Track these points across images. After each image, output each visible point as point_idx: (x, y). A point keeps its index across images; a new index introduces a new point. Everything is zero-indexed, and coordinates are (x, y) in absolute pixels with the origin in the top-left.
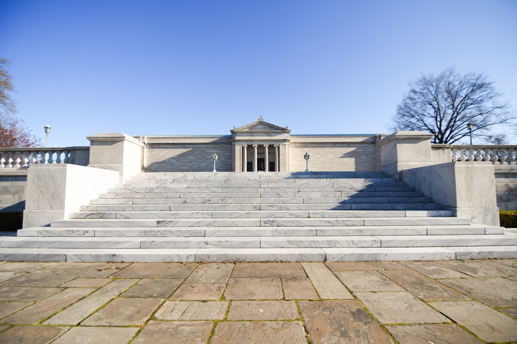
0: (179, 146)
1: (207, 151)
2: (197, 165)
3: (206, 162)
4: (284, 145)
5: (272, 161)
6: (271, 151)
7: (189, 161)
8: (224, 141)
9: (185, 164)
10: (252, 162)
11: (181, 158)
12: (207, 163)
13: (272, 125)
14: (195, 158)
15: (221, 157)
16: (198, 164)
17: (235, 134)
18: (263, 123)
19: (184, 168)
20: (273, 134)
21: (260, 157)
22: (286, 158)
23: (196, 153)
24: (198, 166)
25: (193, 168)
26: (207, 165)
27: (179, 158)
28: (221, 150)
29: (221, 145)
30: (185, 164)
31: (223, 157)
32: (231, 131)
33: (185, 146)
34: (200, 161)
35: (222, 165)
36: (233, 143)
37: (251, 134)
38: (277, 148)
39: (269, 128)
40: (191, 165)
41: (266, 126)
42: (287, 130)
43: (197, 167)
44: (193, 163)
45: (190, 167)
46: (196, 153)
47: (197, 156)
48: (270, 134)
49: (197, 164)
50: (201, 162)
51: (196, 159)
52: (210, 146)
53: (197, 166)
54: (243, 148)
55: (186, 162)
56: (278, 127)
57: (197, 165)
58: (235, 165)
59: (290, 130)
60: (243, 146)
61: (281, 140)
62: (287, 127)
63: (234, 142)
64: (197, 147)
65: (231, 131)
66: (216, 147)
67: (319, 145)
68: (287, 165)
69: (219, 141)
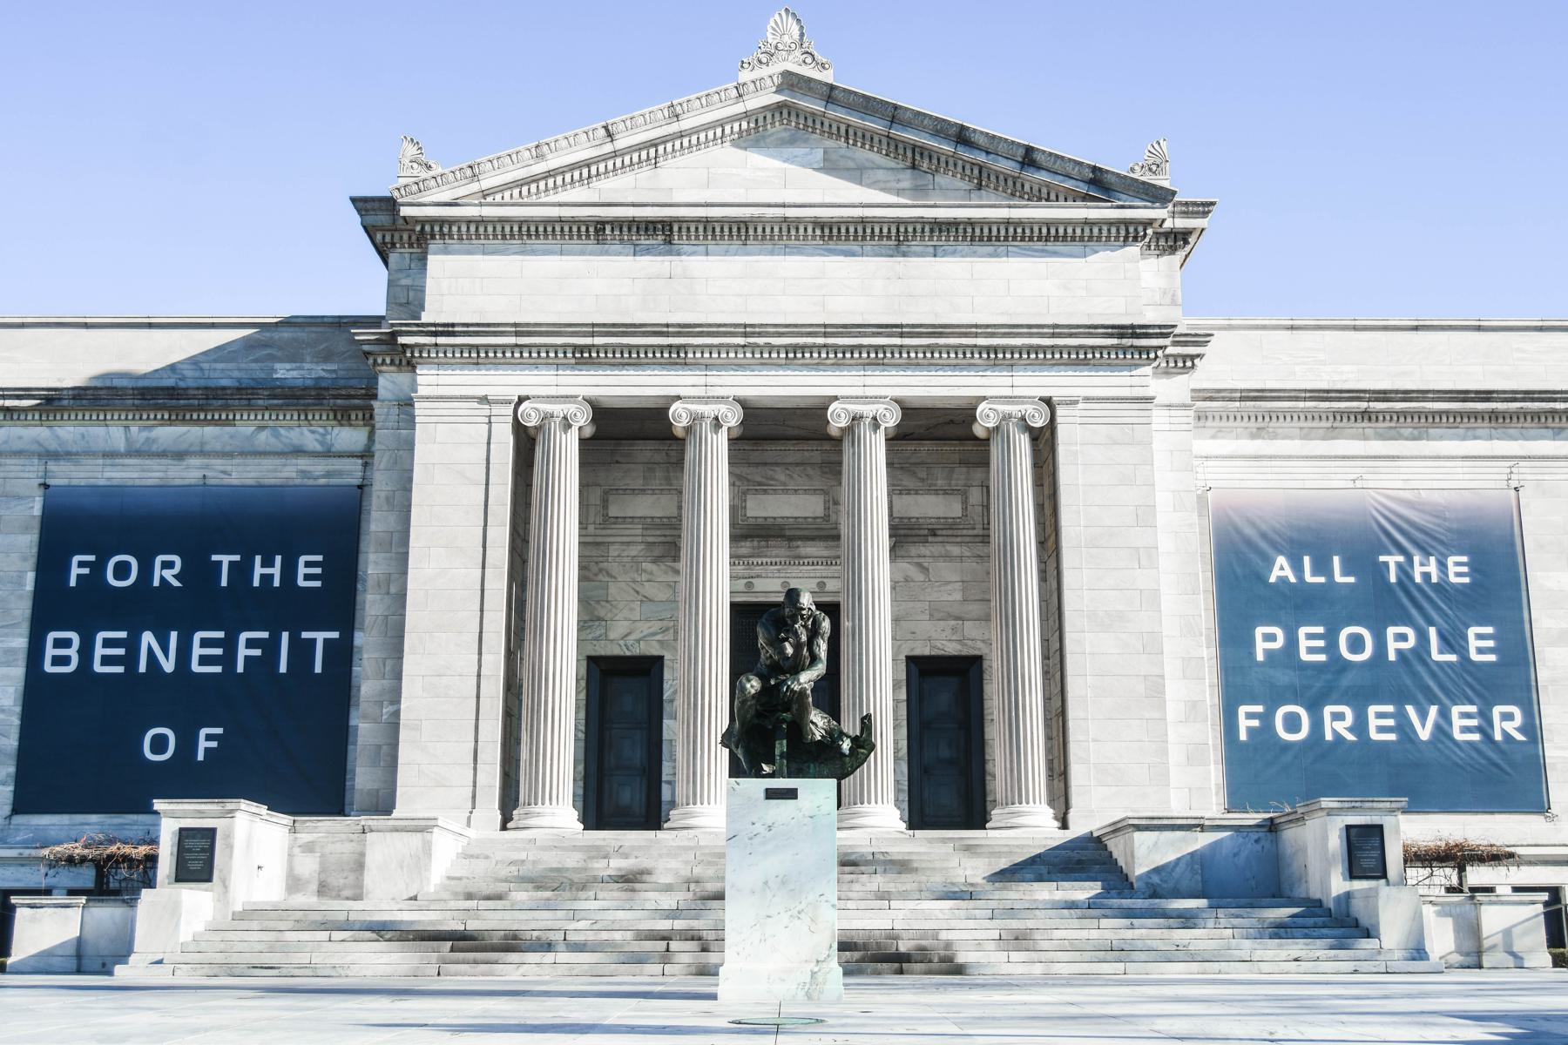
4: (1129, 412)
5: (952, 649)
6: (929, 507)
8: (284, 372)
10: (658, 661)
13: (941, 128)
21: (769, 588)
22: (1155, 594)
29: (245, 428)
32: (361, 204)
36: (388, 383)
38: (1022, 446)
39: (907, 179)
41: (864, 155)
52: (99, 431)
54: (527, 443)
56: (1029, 158)
58: (395, 696)
59: (1204, 208)
63: (407, 361)
65: (361, 204)
69: (226, 375)
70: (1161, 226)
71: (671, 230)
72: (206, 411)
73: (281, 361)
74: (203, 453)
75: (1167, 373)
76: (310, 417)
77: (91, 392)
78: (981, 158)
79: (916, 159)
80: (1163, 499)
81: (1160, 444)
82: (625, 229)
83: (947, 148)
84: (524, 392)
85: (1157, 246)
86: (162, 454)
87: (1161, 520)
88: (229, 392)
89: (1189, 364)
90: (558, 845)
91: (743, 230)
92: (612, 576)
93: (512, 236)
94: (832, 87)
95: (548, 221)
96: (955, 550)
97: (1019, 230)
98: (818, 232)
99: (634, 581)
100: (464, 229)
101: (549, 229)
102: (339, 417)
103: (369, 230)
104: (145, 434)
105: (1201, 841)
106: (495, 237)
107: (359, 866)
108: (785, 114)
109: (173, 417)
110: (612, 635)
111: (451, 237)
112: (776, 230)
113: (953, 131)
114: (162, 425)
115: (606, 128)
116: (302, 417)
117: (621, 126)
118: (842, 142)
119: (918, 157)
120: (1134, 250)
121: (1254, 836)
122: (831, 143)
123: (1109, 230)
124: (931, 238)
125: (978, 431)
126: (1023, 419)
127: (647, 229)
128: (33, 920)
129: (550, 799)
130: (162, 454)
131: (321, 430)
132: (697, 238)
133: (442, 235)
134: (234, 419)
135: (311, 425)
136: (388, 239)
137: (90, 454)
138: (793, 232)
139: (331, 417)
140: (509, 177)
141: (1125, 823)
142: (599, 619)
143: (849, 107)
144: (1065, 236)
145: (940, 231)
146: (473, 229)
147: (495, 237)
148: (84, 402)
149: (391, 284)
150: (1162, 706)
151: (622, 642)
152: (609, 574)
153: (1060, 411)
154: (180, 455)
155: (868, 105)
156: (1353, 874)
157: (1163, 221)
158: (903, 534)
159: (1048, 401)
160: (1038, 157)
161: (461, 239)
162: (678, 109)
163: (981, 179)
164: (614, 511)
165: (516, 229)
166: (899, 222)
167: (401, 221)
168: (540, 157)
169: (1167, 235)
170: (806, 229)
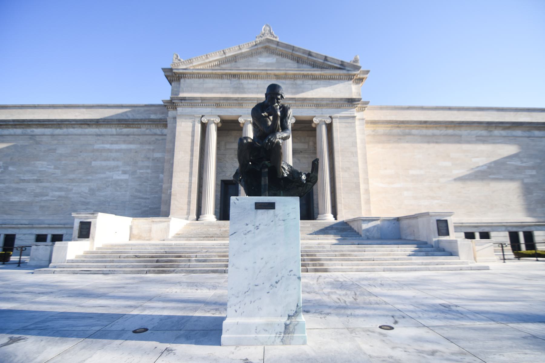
0: (12, 131)
1: (97, 146)
2: (60, 189)
3: (88, 181)
4: (350, 120)
7: (35, 178)
8: (153, 117)
9: (22, 185)
11: (11, 168)
12: (93, 185)
13: (304, 52)
14: (56, 168)
15: (140, 164)
16: (64, 186)
17: (180, 84)
18: (273, 46)
19: (16, 199)
20: (311, 82)
22: (357, 164)
23: (61, 150)
24: (63, 194)
25: (44, 198)
26: (91, 190)
27: (6, 168)
28: (141, 143)
29: (143, 129)
30: (22, 185)
31: (146, 163)
32: (164, 70)
33: (29, 131)
34: (72, 176)
35: (140, 191)
37: (235, 81)
38: (324, 129)
39: (296, 65)
40: (38, 191)
41: (285, 60)
42: (358, 68)
43: (60, 197)
44: (47, 185)
45: (36, 195)
46: (61, 150)
47: (63, 162)
48: (299, 82)
49: (59, 185)
50: (72, 180)
51: (57, 171)
53: (57, 193)
54: (204, 127)
55: (24, 181)
56: (326, 59)
57: (60, 189)
58: (170, 188)
59: (367, 72)
60: (205, 120)
61: (337, 100)
62: (356, 61)
64: (68, 135)
65: (164, 70)
66: (128, 135)
67: (444, 131)
68: (362, 187)
70: (357, 76)
71: (239, 76)
72: (134, 125)
73: (152, 114)
74: (134, 135)
75: (358, 111)
76: (158, 126)
77: (106, 120)
78: (315, 59)
79: (298, 60)
80: (358, 141)
81: (358, 128)
82: (228, 76)
83: (306, 56)
84: (203, 114)
85: (356, 82)
86: (124, 135)
87: (358, 146)
88: (139, 120)
89: (364, 109)
90: (211, 225)
91: (257, 76)
92: (227, 162)
93: (201, 78)
94: (278, 42)
95: (209, 74)
96: (306, 156)
97: (323, 77)
98: (275, 77)
99: (232, 163)
100: (189, 75)
101: (210, 76)
102: (165, 126)
103: (167, 77)
104: (120, 130)
105: (378, 222)
106: (197, 78)
107: (150, 231)
108: (267, 49)
109: (127, 126)
110: (227, 175)
111: (186, 78)
112: (265, 76)
113: (308, 52)
114: (124, 128)
115: (223, 51)
116: (156, 126)
117: (227, 51)
118: (281, 57)
119: (299, 59)
120: (351, 82)
121: (393, 222)
122: (278, 57)
123: (345, 77)
124: (302, 79)
125: (313, 125)
126: (325, 121)
127: (233, 76)
128: (36, 249)
129: (208, 213)
130: (124, 135)
131: (161, 130)
132: (246, 78)
133: (184, 78)
134: (141, 127)
135: (158, 128)
136: (171, 79)
137: (108, 135)
138: (269, 77)
139: (163, 126)
140: (200, 63)
141: (359, 219)
142: (224, 171)
143: (283, 47)
144: (334, 78)
145: (304, 77)
146: (191, 75)
147: (197, 78)
148: (105, 123)
149: (172, 90)
150: (359, 189)
151: (229, 177)
152: (226, 161)
153: (334, 120)
154: (128, 135)
155: (287, 46)
156: (440, 234)
157: (358, 74)
158: (295, 152)
159: (331, 117)
160: (328, 59)
161: (188, 78)
162: (241, 47)
163: (314, 65)
164: (227, 147)
165: (202, 76)
166: (294, 75)
167: (174, 74)
168: (207, 58)
169: (358, 79)
170: (272, 76)
